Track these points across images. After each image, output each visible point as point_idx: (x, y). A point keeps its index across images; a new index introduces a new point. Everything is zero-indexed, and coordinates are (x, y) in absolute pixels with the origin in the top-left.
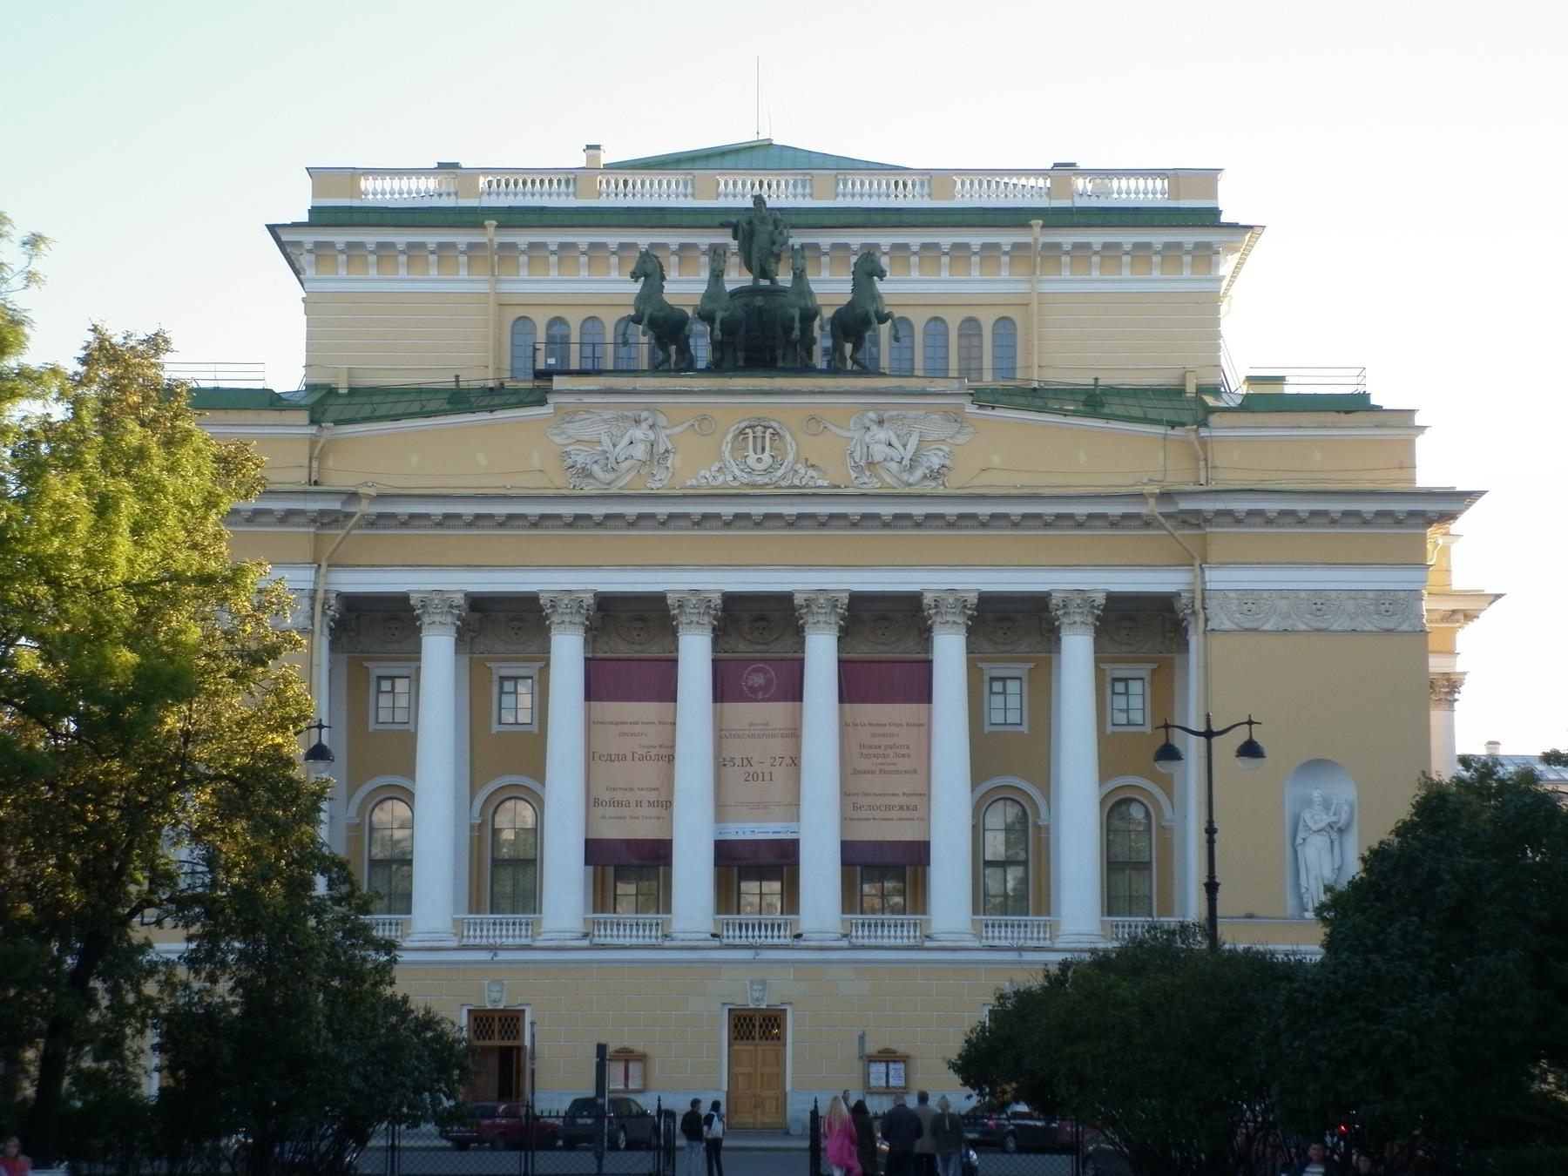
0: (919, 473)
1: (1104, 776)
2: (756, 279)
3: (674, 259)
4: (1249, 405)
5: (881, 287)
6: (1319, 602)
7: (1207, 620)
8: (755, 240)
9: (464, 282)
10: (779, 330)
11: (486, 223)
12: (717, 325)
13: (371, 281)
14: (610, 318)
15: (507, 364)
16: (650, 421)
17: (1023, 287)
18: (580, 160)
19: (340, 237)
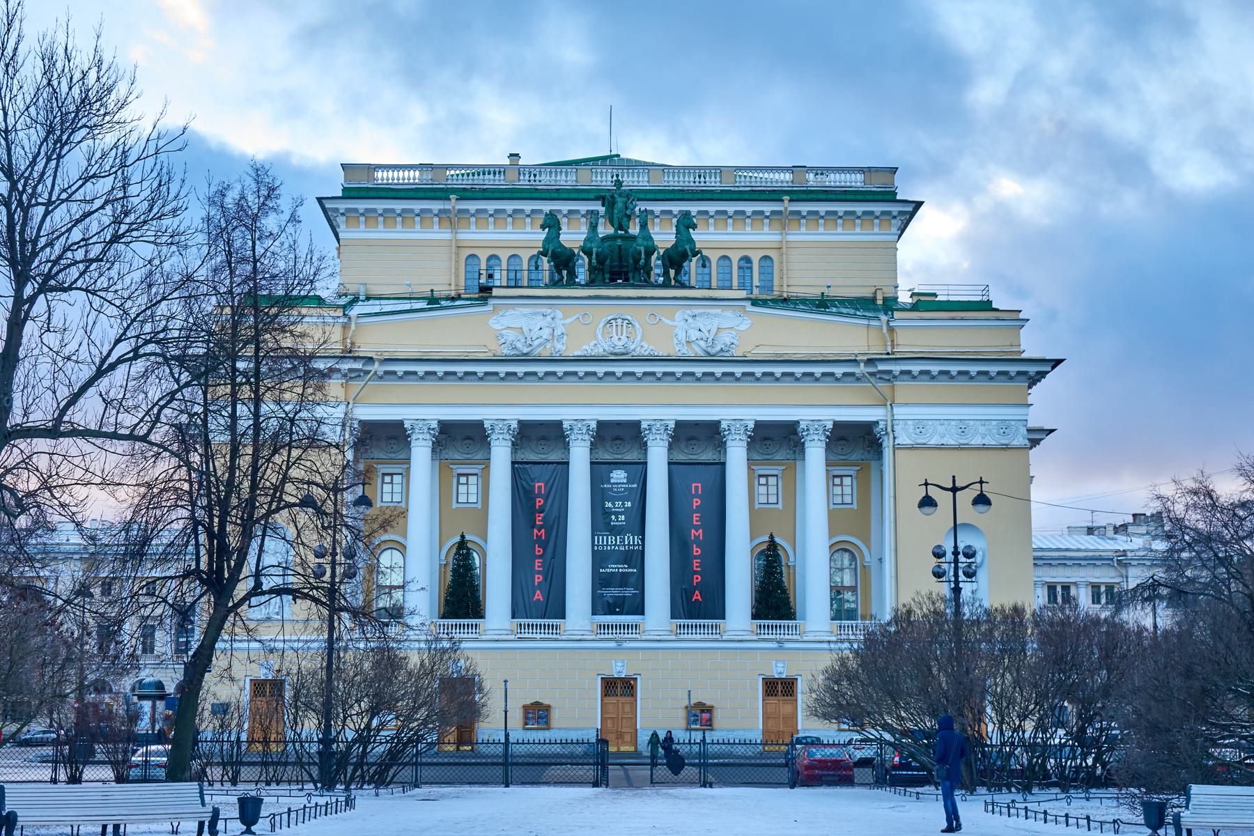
0: (718, 348)
1: (832, 532)
2: (616, 231)
3: (565, 220)
4: (914, 307)
5: (696, 235)
6: (963, 427)
7: (894, 438)
8: (616, 206)
9: (439, 234)
10: (631, 261)
11: (451, 196)
12: (594, 256)
14: (525, 255)
15: (462, 283)
16: (552, 316)
17: (778, 238)
18: (507, 162)
19: (361, 205)
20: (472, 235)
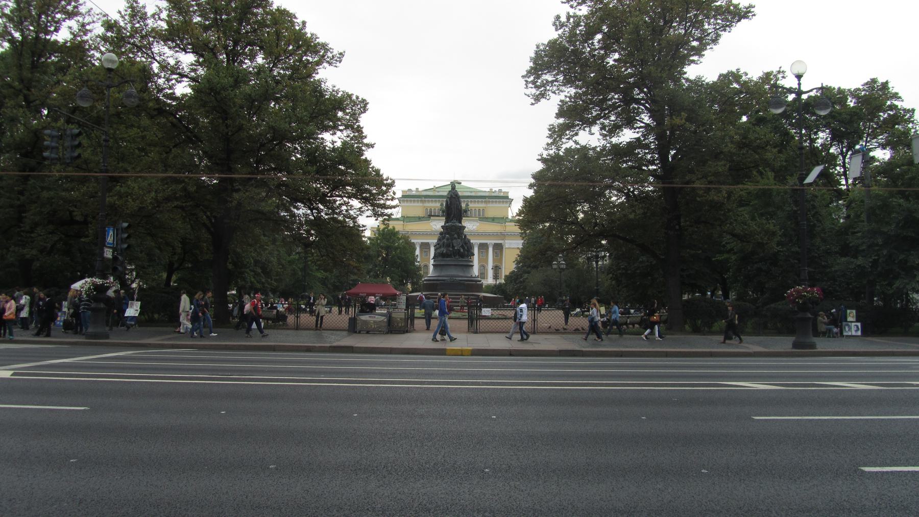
13: (408, 204)
14: (437, 209)
20: (427, 205)
